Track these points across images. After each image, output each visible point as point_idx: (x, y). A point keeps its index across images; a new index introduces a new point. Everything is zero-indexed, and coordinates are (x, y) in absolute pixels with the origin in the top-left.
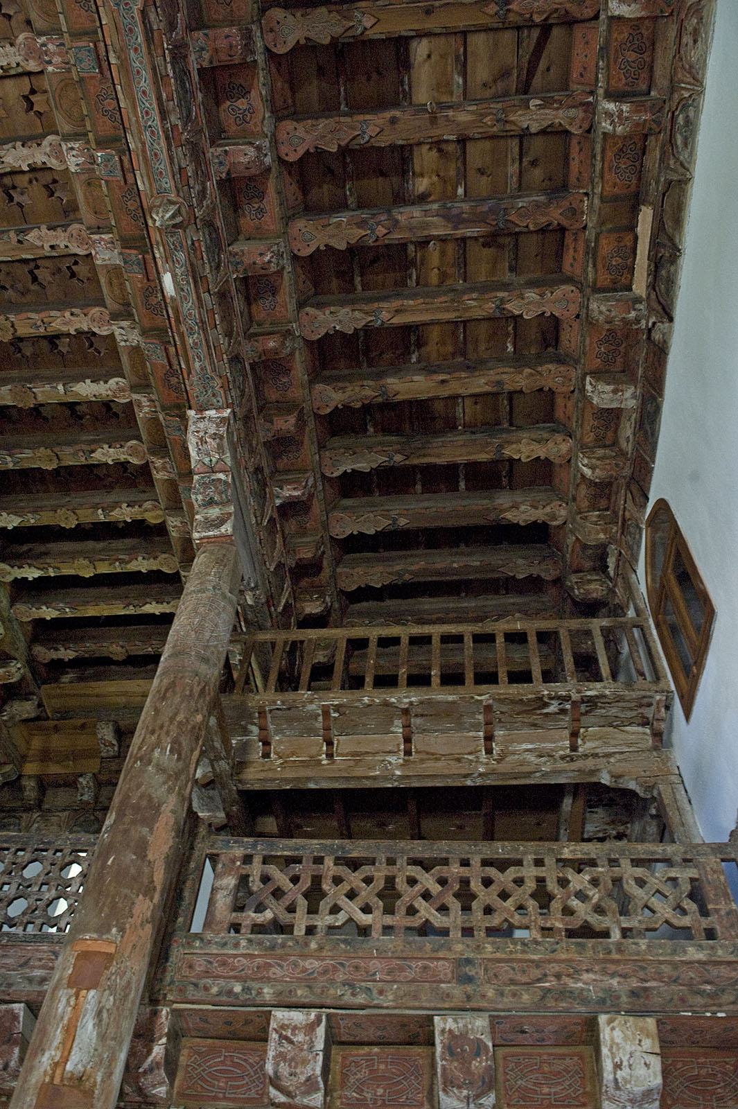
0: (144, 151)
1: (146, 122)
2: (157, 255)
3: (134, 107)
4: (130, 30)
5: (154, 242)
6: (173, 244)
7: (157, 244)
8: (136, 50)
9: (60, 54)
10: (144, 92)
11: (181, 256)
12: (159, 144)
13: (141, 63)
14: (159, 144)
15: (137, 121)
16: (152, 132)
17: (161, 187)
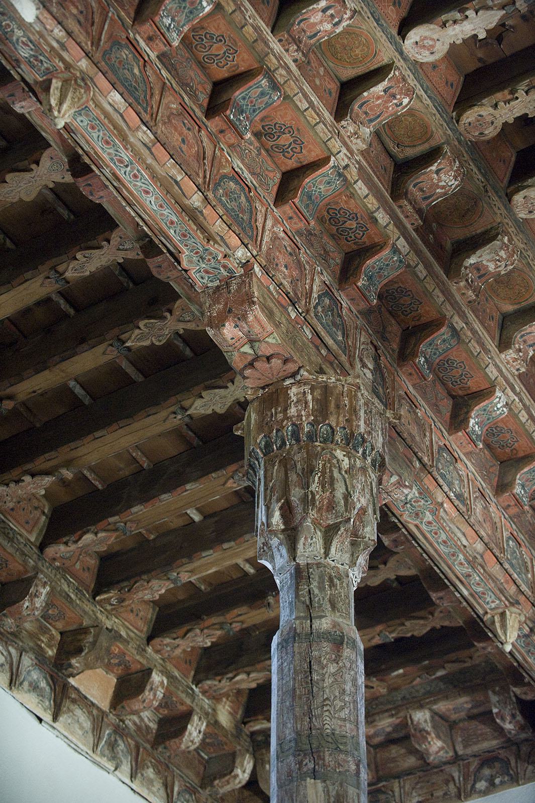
0: (124, 139)
1: (133, 169)
2: (59, 32)
3: (154, 176)
4: (185, 236)
5: (71, 44)
6: (41, 61)
7: (63, 46)
8: (172, 223)
9: (315, 24)
10: (147, 192)
11: (24, 53)
12: (109, 154)
13: (162, 215)
14: (109, 154)
15: (144, 161)
16: (121, 161)
17: (87, 115)
